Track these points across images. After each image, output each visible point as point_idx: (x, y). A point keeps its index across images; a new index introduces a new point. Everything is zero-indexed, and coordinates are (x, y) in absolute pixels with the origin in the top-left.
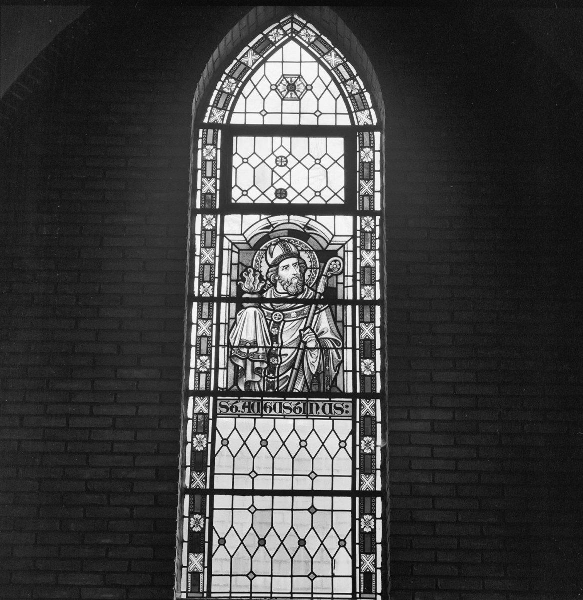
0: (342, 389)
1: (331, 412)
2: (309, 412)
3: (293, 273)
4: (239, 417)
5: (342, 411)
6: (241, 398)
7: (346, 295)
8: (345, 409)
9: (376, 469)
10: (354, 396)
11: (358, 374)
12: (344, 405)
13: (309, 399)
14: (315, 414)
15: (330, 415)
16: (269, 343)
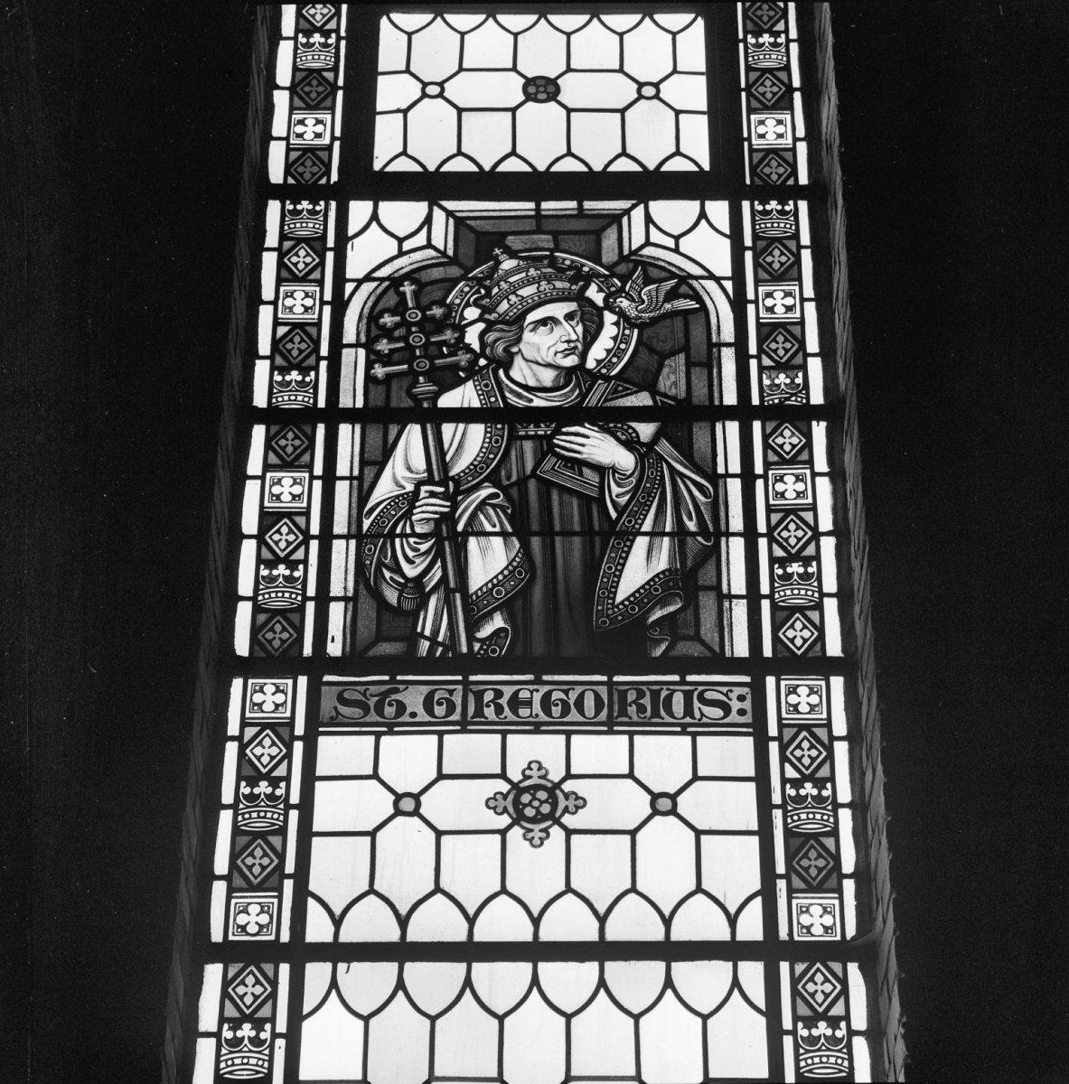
0: (717, 649)
1: (689, 710)
2: (615, 714)
3: (564, 339)
4: (391, 733)
5: (727, 709)
6: (399, 678)
7: (716, 395)
8: (736, 705)
9: (843, 876)
10: (756, 666)
11: (765, 604)
12: (734, 696)
13: (616, 679)
14: (635, 718)
15: (688, 720)
16: (494, 526)
